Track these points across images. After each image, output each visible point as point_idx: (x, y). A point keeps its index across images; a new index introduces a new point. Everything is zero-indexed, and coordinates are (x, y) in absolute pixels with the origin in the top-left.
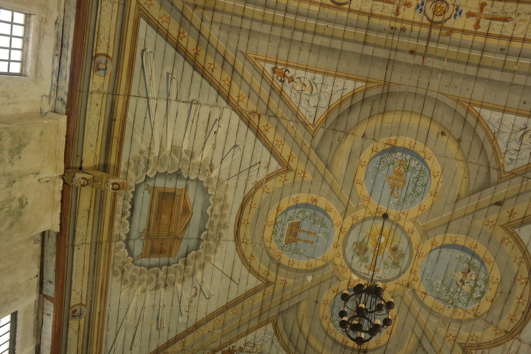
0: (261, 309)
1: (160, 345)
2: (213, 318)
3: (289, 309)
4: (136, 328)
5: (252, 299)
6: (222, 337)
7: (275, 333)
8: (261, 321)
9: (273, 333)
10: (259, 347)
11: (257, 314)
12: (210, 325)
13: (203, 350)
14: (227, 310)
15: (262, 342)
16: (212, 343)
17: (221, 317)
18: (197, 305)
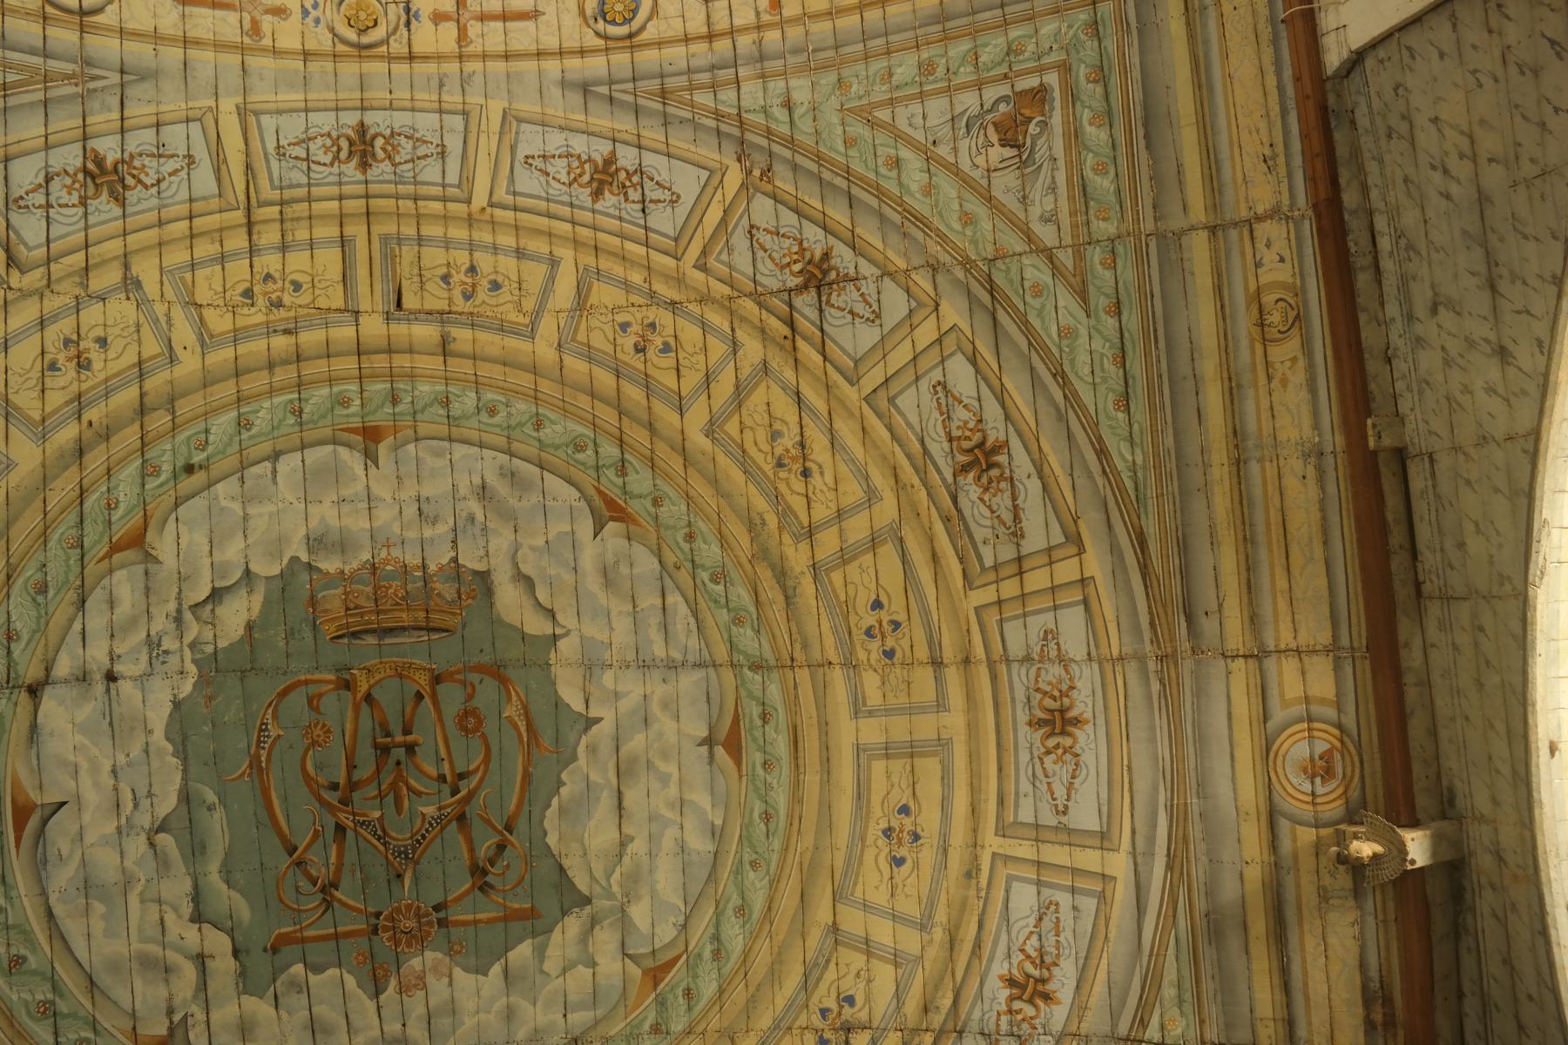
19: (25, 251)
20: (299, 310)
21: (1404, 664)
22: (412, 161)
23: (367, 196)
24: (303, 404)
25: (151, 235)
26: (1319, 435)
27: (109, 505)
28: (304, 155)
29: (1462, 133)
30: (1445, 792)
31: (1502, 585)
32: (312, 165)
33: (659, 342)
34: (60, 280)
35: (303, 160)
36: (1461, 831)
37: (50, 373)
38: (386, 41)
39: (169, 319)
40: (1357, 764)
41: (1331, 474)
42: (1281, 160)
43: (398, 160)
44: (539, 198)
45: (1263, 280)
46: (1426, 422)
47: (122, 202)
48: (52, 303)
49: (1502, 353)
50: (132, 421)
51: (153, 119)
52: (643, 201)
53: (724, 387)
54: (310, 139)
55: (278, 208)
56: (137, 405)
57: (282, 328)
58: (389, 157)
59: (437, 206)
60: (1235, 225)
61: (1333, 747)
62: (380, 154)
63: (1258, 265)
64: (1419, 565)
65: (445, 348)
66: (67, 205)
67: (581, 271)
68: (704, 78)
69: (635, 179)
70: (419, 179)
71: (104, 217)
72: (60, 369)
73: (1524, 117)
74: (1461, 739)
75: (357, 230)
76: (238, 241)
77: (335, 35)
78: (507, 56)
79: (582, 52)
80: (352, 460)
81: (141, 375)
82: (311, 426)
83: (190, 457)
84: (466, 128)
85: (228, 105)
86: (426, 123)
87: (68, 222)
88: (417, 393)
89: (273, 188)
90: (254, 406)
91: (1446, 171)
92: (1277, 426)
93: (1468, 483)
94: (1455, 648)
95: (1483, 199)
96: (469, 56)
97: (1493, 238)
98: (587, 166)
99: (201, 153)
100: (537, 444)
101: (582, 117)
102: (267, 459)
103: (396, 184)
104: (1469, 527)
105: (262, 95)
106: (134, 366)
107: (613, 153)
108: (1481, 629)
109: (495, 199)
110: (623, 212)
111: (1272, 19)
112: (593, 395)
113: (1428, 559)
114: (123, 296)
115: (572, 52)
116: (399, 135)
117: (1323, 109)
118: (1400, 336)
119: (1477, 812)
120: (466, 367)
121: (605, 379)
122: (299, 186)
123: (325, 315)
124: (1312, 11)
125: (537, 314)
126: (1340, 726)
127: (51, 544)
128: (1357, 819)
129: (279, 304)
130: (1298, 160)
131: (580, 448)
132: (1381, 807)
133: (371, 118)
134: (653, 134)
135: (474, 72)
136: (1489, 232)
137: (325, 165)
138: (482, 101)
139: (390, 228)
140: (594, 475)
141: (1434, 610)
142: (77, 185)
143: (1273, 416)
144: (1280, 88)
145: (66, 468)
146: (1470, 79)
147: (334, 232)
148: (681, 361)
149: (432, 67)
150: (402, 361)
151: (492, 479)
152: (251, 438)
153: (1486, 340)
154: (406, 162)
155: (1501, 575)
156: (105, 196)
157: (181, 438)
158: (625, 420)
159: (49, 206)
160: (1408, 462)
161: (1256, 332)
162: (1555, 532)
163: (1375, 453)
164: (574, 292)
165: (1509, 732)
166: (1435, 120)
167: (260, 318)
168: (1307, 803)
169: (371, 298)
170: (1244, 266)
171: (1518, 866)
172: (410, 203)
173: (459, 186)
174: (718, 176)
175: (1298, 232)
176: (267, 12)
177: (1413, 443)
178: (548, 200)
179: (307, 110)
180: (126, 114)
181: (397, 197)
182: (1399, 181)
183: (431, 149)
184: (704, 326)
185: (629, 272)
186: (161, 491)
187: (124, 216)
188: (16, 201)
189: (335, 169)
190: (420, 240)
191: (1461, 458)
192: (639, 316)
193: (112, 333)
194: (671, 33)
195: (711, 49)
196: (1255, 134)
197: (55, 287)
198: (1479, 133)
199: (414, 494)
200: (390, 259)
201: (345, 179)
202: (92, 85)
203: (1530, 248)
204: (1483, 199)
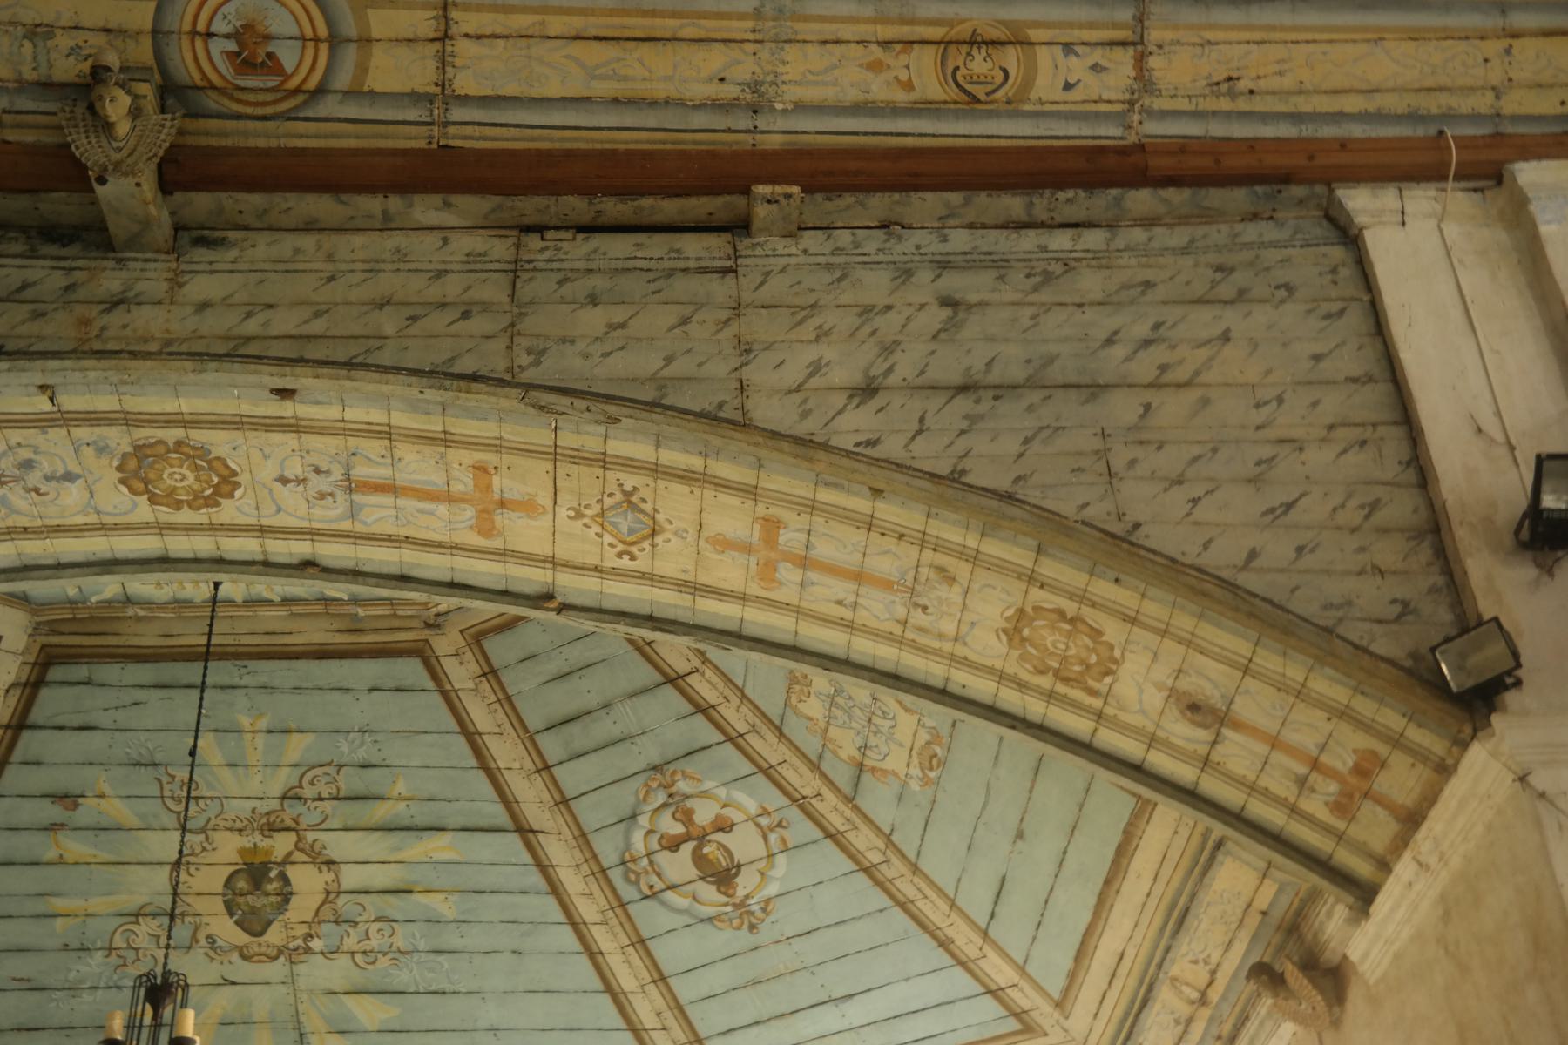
21: (417, 198)
26: (785, 111)
29: (1197, 373)
30: (218, 234)
31: (529, 352)
36: (158, 251)
40: (260, 111)
41: (720, 121)
42: (1225, 104)
45: (1043, 53)
46: (783, 270)
49: (867, 391)
60: (1140, 19)
61: (288, 77)
63: (1068, 48)
64: (569, 235)
73: (1195, 459)
74: (300, 266)
91: (1147, 343)
92: (810, 48)
93: (685, 321)
94: (440, 274)
95: (1094, 389)
97: (1035, 397)
104: (619, 315)
108: (466, 315)
111: (1450, 117)
113: (578, 249)
117: (1285, 178)
118: (918, 247)
119: (187, 277)
124: (1444, 178)
126: (321, 91)
128: (170, 102)
130: (1218, 129)
132: (190, 140)
136: (1046, 392)
141: (500, 248)
143: (825, 42)
144: (1339, 117)
146: (1271, 393)
153: (890, 370)
155: (543, 352)
160: (727, 236)
161: (963, 31)
162: (601, 429)
163: (746, 191)
165: (309, 337)
166: (1226, 337)
168: (194, 23)
170: (1070, 25)
171: (103, 328)
175: (1107, 116)
177: (754, 246)
182: (1149, 275)
191: (725, 314)
196: (1277, 68)
198: (1193, 395)
203: (1012, 445)
204: (1094, 389)
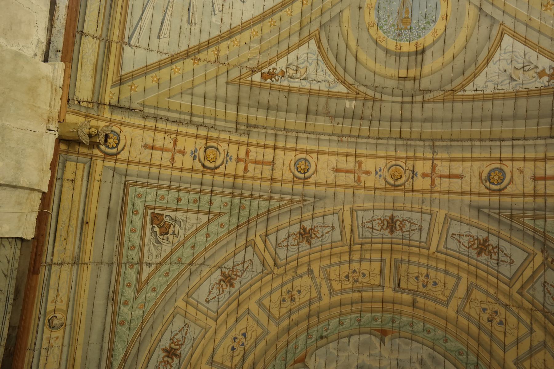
0: (301, 22)
1: (191, 46)
2: (250, 27)
3: (331, 21)
4: (166, 11)
5: (290, 9)
6: (260, 53)
7: (319, 51)
8: (302, 37)
9: (317, 52)
10: (303, 71)
11: (298, 28)
12: (246, 35)
13: (240, 67)
14: (264, 20)
15: (305, 64)
16: (249, 59)
17: (257, 28)
18: (231, 7)
19: (279, 260)
20: (364, 284)
22: (409, 231)
23: (392, 243)
24: (361, 318)
25: (318, 255)
27: (296, 347)
28: (371, 226)
32: (373, 230)
33: (498, 319)
34: (289, 270)
35: (371, 228)
37: (283, 302)
38: (404, 184)
39: (320, 283)
43: (404, 230)
44: (456, 251)
47: (309, 243)
48: (286, 278)
50: (306, 320)
51: (322, 214)
52: (498, 260)
53: (525, 347)
54: (374, 220)
55: (360, 246)
56: (307, 314)
57: (357, 290)
58: (401, 229)
59: (416, 250)
62: (398, 228)
65: (414, 305)
66: (293, 245)
67: (469, 283)
68: (530, 213)
69: (496, 250)
70: (411, 238)
71: (304, 248)
72: (286, 301)
75: (386, 256)
76: (346, 258)
77: (386, 181)
78: (449, 193)
79: (479, 194)
80: (376, 341)
81: (310, 304)
82: (363, 327)
83: (322, 334)
84: (430, 220)
85: (347, 208)
86: (416, 217)
87: (293, 250)
88: (401, 320)
89: (359, 238)
90: (345, 317)
96: (435, 192)
98: (476, 241)
99: (337, 226)
100: (444, 348)
101: (476, 221)
102: (347, 337)
103: (403, 239)
105: (359, 204)
106: (308, 301)
107: (488, 238)
109: (439, 249)
110: (489, 263)
112: (468, 334)
114: (307, 276)
115: (475, 194)
116: (406, 221)
120: (420, 313)
121: (474, 329)
122: (368, 238)
123: (372, 287)
125: (450, 297)
127: (277, 359)
129: (357, 281)
131: (461, 354)
133: (397, 214)
134: (505, 233)
135: (436, 198)
137: (378, 230)
138: (437, 210)
139: (398, 256)
140: (465, 366)
142: (297, 238)
145: (284, 334)
147: (379, 256)
148: (507, 330)
149: (420, 195)
150: (398, 307)
151: (425, 357)
152: (343, 328)
154: (407, 231)
156: (305, 240)
157: (320, 326)
158: (480, 347)
159: (288, 245)
164: (465, 291)
167: (350, 286)
169: (389, 282)
172: (407, 247)
173: (426, 243)
174: (532, 257)
176: (363, 173)
178: (459, 253)
179: (374, 210)
180: (315, 212)
181: (402, 245)
183: (417, 227)
184: (519, 318)
185: (489, 288)
186: (312, 344)
187: (310, 248)
188: (279, 244)
189: (381, 232)
190: (409, 262)
192: (491, 307)
193: (303, 288)
194: (517, 192)
195: (534, 201)
197: (287, 273)
199: (396, 357)
200: (397, 268)
201: (385, 236)
202: (305, 203)
